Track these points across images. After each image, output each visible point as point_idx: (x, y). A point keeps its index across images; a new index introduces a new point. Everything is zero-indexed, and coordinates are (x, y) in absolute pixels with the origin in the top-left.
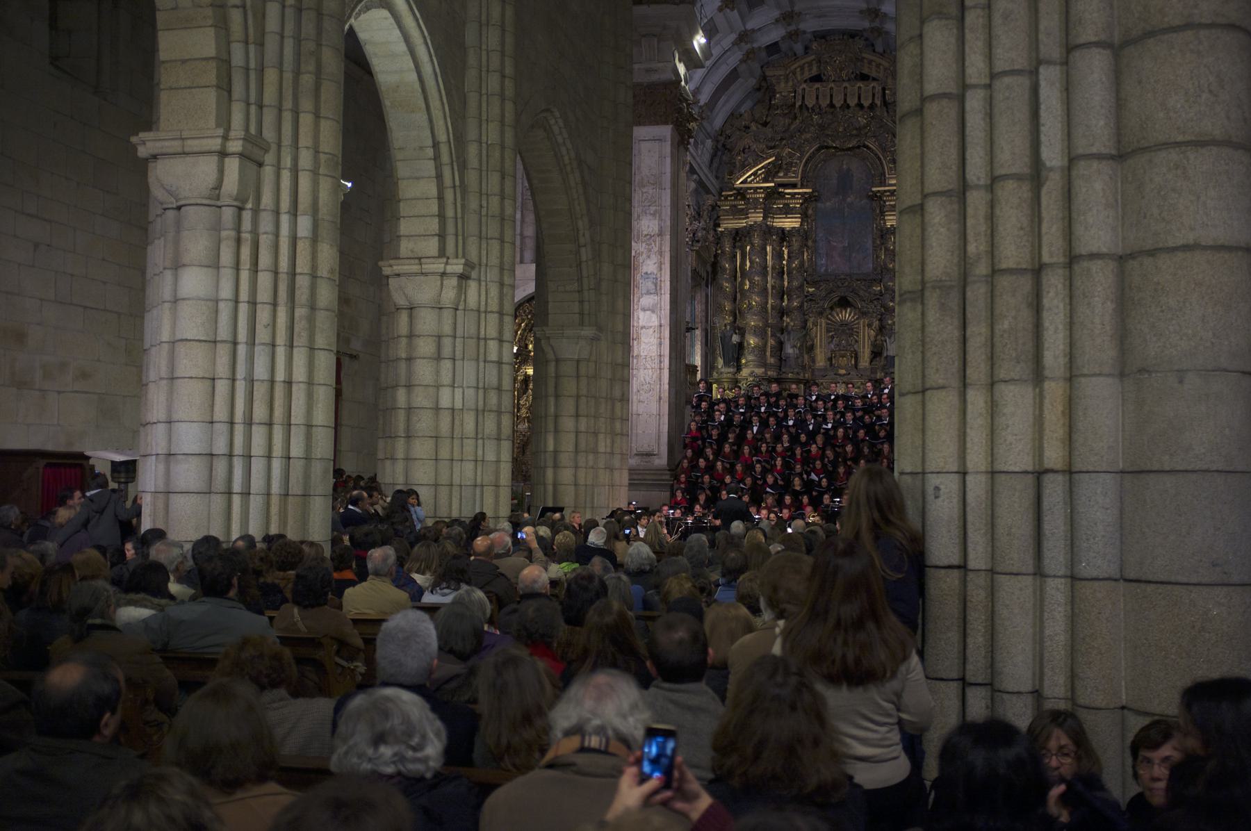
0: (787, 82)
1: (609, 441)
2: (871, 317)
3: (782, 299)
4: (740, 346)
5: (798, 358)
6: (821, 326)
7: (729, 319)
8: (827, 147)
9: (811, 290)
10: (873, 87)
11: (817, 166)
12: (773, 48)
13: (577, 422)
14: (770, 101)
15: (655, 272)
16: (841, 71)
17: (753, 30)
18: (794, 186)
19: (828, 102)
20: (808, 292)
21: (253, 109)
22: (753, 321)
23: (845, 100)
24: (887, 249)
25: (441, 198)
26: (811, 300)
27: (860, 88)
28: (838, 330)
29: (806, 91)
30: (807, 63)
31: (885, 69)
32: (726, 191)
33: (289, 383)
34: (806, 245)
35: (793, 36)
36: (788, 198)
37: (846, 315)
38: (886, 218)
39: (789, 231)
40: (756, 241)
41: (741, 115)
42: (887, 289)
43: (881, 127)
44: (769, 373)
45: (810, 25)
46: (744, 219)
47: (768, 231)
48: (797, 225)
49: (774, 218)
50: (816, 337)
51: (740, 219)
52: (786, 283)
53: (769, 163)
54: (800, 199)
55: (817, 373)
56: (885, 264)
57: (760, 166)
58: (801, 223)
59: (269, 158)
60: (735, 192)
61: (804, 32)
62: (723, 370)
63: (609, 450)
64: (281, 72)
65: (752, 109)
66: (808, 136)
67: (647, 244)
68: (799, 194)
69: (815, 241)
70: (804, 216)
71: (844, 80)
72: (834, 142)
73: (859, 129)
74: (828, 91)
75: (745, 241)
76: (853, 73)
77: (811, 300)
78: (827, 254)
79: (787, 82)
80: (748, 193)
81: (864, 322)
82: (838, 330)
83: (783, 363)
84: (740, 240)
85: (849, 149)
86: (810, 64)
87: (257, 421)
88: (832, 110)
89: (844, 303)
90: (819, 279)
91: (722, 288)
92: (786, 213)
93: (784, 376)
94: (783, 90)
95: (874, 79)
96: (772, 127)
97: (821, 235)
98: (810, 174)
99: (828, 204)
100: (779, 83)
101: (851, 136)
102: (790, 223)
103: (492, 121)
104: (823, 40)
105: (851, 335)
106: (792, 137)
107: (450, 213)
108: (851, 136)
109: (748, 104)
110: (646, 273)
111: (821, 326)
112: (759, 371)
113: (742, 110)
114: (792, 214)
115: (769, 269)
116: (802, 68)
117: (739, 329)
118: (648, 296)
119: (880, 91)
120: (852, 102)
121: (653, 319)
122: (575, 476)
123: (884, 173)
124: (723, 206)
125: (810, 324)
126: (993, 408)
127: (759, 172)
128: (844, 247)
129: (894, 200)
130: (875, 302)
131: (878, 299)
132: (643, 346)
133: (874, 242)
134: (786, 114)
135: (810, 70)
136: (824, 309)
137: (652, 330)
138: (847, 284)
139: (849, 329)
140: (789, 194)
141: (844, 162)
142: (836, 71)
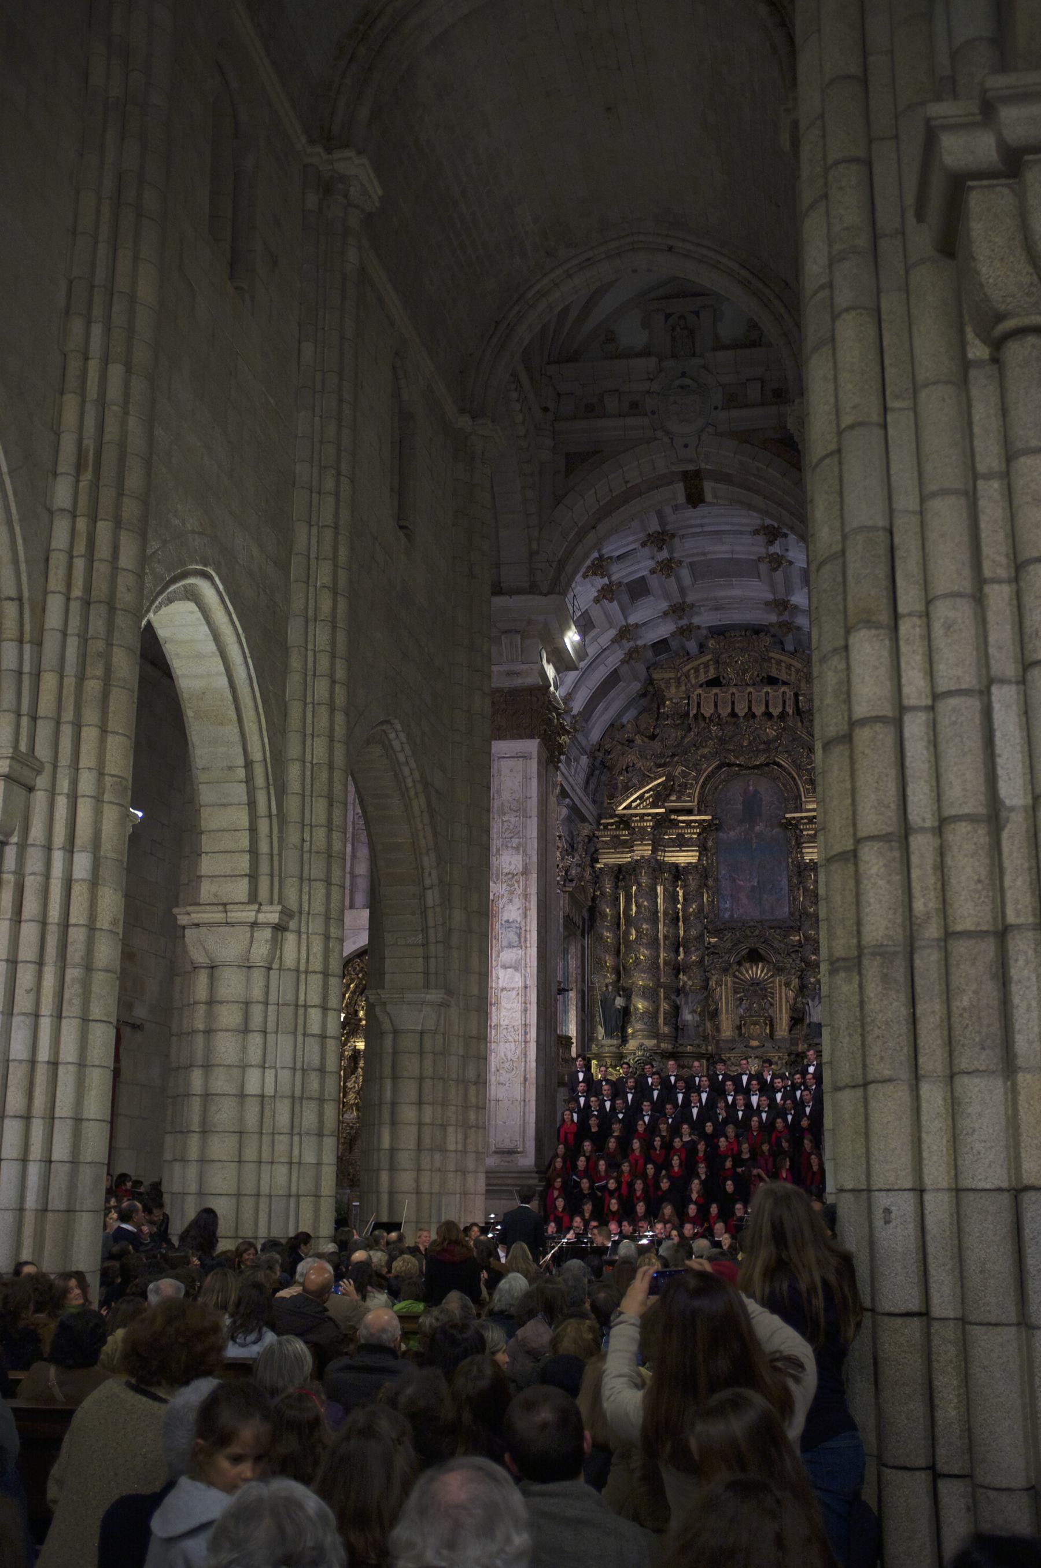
0: (678, 687)
1: (460, 1137)
2: (789, 973)
3: (677, 953)
4: (626, 1012)
5: (698, 1026)
6: (726, 985)
7: (611, 978)
8: (729, 765)
9: (713, 940)
10: (784, 693)
11: (716, 789)
12: (661, 646)
13: (420, 1110)
14: (659, 709)
15: (519, 920)
16: (744, 674)
17: (637, 625)
18: (689, 812)
19: (729, 710)
20: (709, 943)
21: (25, 721)
22: (640, 980)
23: (750, 708)
25: (253, 830)
26: (713, 953)
27: (767, 693)
29: (702, 697)
31: (797, 671)
32: (606, 818)
33: (54, 1064)
34: (706, 885)
35: (685, 631)
36: (683, 827)
37: (757, 972)
38: (804, 851)
40: (644, 880)
41: (623, 726)
42: (807, 938)
43: (794, 740)
44: (662, 1045)
45: (705, 619)
46: (628, 853)
47: (658, 868)
48: (694, 860)
49: (665, 851)
50: (721, 998)
51: (623, 853)
52: (682, 933)
53: (658, 784)
54: (696, 827)
55: (722, 1045)
56: (804, 908)
57: (647, 788)
58: (699, 857)
59: (42, 782)
60: (616, 819)
61: (699, 627)
62: (604, 1042)
63: (460, 1147)
64: (62, 677)
65: (636, 718)
66: (706, 751)
67: (508, 885)
68: (695, 821)
69: (716, 880)
70: (703, 850)
71: (747, 685)
72: (737, 758)
73: (767, 743)
74: (729, 697)
75: (630, 880)
76: (758, 675)
77: (713, 953)
78: (731, 896)
79: (678, 687)
80: (633, 821)
81: (780, 981)
82: (748, 990)
83: (680, 1032)
84: (624, 878)
85: (756, 767)
86: (706, 665)
87: (11, 1114)
88: (733, 720)
89: (754, 957)
90: (722, 927)
91: (602, 938)
92: (680, 846)
93: (681, 1049)
94: (674, 695)
95: (785, 683)
96: (662, 741)
97: (723, 872)
98: (710, 798)
99: (732, 834)
100: (669, 688)
101: (758, 751)
102: (686, 857)
103: (318, 736)
104: (722, 637)
106: (686, 753)
107: (264, 847)
109: (632, 713)
110: (508, 921)
111: (726, 985)
112: (651, 1043)
113: (625, 720)
114: (688, 846)
115: (661, 915)
116: (696, 670)
117: (624, 989)
118: (510, 950)
120: (759, 710)
121: (517, 980)
122: (417, 1181)
123: (800, 796)
124: (602, 836)
125: (712, 983)
126: (954, 1106)
127: (647, 795)
128: (753, 887)
129: (812, 829)
130: (794, 956)
131: (797, 951)
132: (504, 1013)
133: (789, 881)
134: (679, 724)
135: (706, 672)
136: (730, 965)
137: (515, 993)
138: (757, 932)
139: (761, 990)
140: (683, 821)
141: (751, 783)
142: (738, 673)
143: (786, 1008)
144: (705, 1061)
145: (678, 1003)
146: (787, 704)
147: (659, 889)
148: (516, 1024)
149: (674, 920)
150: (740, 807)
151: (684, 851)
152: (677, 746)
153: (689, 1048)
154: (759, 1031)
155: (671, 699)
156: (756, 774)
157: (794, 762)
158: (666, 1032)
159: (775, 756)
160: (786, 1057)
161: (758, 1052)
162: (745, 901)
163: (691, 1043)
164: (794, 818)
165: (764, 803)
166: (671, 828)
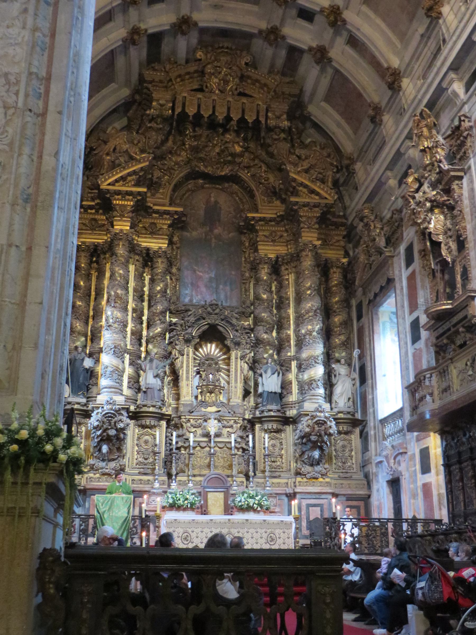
11: (184, 195)
24: (258, 281)
28: (204, 364)
29: (187, 99)
30: (188, 73)
32: (87, 200)
36: (156, 218)
38: (259, 247)
39: (155, 252)
50: (182, 367)
51: (100, 234)
53: (142, 169)
55: (181, 409)
58: (168, 244)
62: (70, 400)
66: (180, 159)
70: (171, 243)
72: (206, 167)
73: (233, 155)
76: (236, 89)
81: (236, 355)
82: (204, 364)
84: (98, 256)
90: (183, 308)
92: (152, 233)
99: (194, 233)
105: (219, 370)
108: (225, 163)
111: (188, 355)
114: (159, 235)
119: (265, 111)
127: (129, 178)
129: (267, 230)
134: (161, 129)
138: (217, 311)
140: (157, 212)
141: (212, 195)
143: (241, 378)
144: (164, 423)
145: (143, 367)
146: (261, 114)
147: (132, 268)
148: (16, 70)
149: (141, 298)
150: (202, 212)
151: (155, 238)
152: (158, 148)
153: (151, 409)
154: (214, 399)
155: (158, 100)
156: (217, 189)
157: (253, 176)
158: (129, 395)
159: (237, 171)
160: (241, 422)
161: (217, 415)
162: (203, 289)
163: (154, 404)
164: (254, 217)
165: (222, 212)
166: (145, 217)
